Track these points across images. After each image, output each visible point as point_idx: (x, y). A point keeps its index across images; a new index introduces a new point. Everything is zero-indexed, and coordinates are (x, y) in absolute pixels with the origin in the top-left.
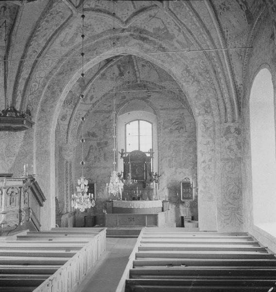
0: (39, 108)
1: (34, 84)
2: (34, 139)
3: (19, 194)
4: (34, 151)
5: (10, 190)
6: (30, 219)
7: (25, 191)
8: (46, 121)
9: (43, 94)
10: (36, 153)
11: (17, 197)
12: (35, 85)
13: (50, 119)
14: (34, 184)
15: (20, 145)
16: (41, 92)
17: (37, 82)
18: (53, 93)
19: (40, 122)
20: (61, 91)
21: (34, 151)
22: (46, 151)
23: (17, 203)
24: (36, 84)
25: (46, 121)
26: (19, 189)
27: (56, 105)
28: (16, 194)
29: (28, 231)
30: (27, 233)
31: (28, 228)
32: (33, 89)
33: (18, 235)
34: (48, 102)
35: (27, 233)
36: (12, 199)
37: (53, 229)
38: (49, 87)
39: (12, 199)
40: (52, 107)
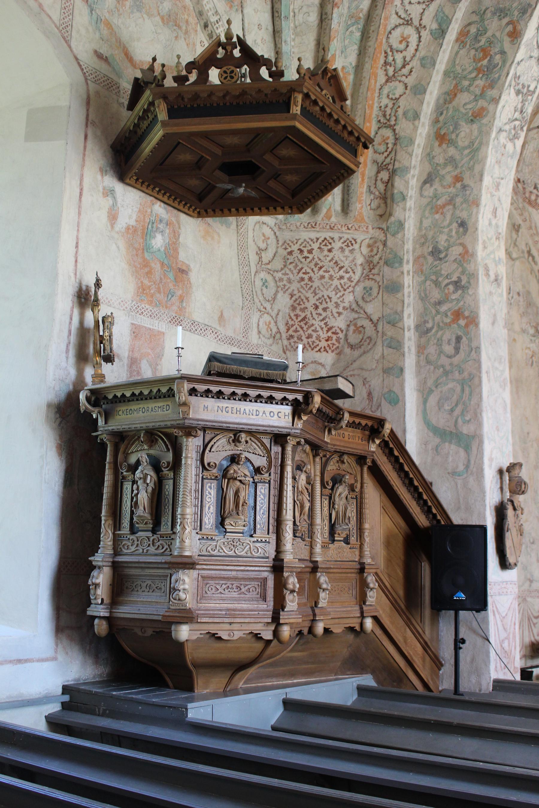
0: (423, 131)
1: (398, 31)
2: (408, 267)
3: (274, 476)
4: (409, 320)
5: (220, 451)
6: (369, 623)
7: (337, 480)
8: (458, 179)
9: (441, 65)
10: (417, 327)
11: (262, 489)
12: (404, 39)
13: (471, 169)
14: (385, 445)
15: (349, 298)
16: (428, 63)
17: (408, 22)
18: (485, 52)
19: (429, 191)
20: (515, 35)
21: (409, 320)
22: (458, 314)
23: (262, 518)
24: (409, 31)
25: (458, 179)
26: (276, 449)
27: (496, 101)
28: (258, 471)
29: (368, 680)
30: (362, 690)
31: (354, 664)
32: (399, 58)
33: (298, 694)
34: (464, 98)
35: (362, 690)
36: (231, 495)
37: (500, 685)
38: (463, 35)
39: (231, 495)
40: (477, 116)
